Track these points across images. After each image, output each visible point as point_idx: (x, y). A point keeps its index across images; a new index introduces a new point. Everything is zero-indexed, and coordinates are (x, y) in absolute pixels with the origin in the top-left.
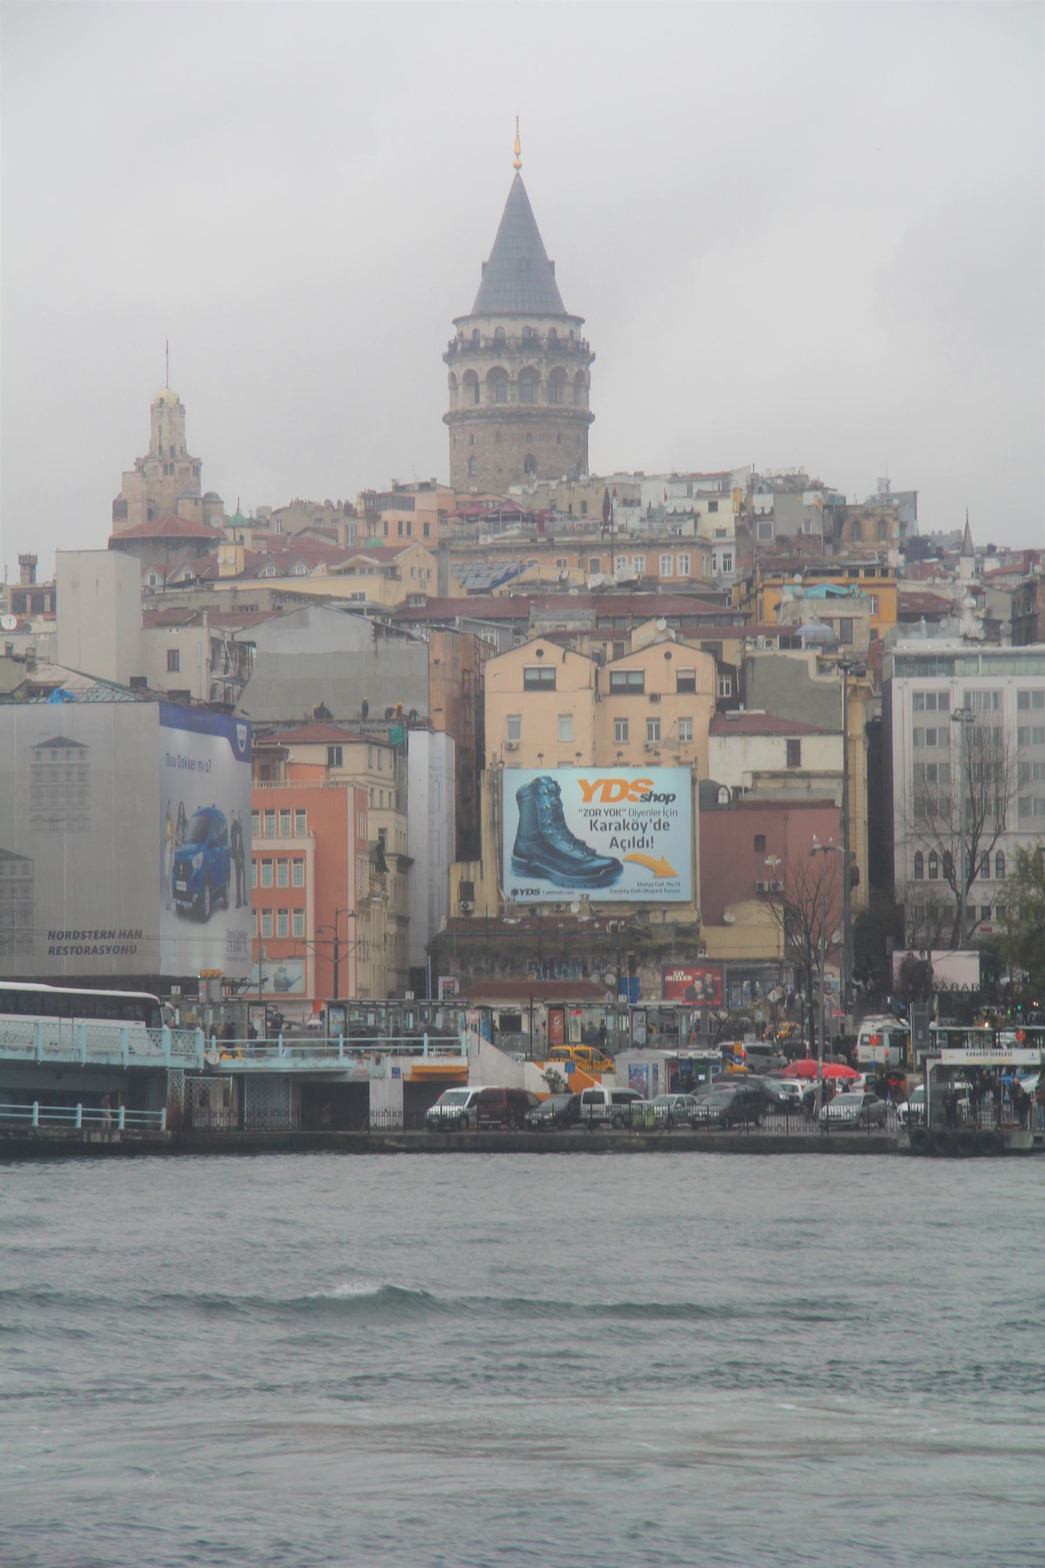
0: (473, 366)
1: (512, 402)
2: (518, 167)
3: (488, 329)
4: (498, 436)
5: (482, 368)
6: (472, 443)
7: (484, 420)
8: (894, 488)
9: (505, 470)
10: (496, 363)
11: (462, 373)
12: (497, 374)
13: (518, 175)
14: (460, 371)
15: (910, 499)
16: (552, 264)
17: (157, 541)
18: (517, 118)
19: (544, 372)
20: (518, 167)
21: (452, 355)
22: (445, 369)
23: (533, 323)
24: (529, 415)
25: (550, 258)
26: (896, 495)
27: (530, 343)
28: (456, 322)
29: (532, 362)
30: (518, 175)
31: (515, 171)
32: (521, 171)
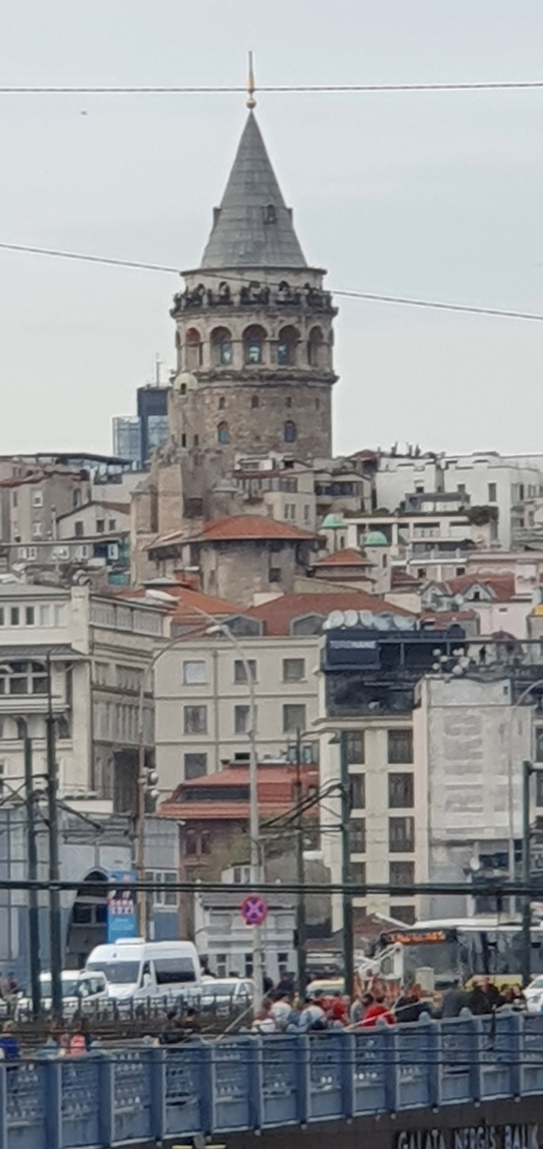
0: (225, 325)
2: (251, 106)
6: (221, 407)
7: (240, 383)
9: (263, 438)
10: (253, 320)
11: (210, 330)
13: (251, 117)
16: (290, 211)
17: (260, 543)
18: (250, 53)
20: (251, 106)
24: (291, 378)
25: (288, 205)
28: (184, 274)
29: (291, 321)
30: (251, 117)
31: (248, 110)
32: (255, 110)
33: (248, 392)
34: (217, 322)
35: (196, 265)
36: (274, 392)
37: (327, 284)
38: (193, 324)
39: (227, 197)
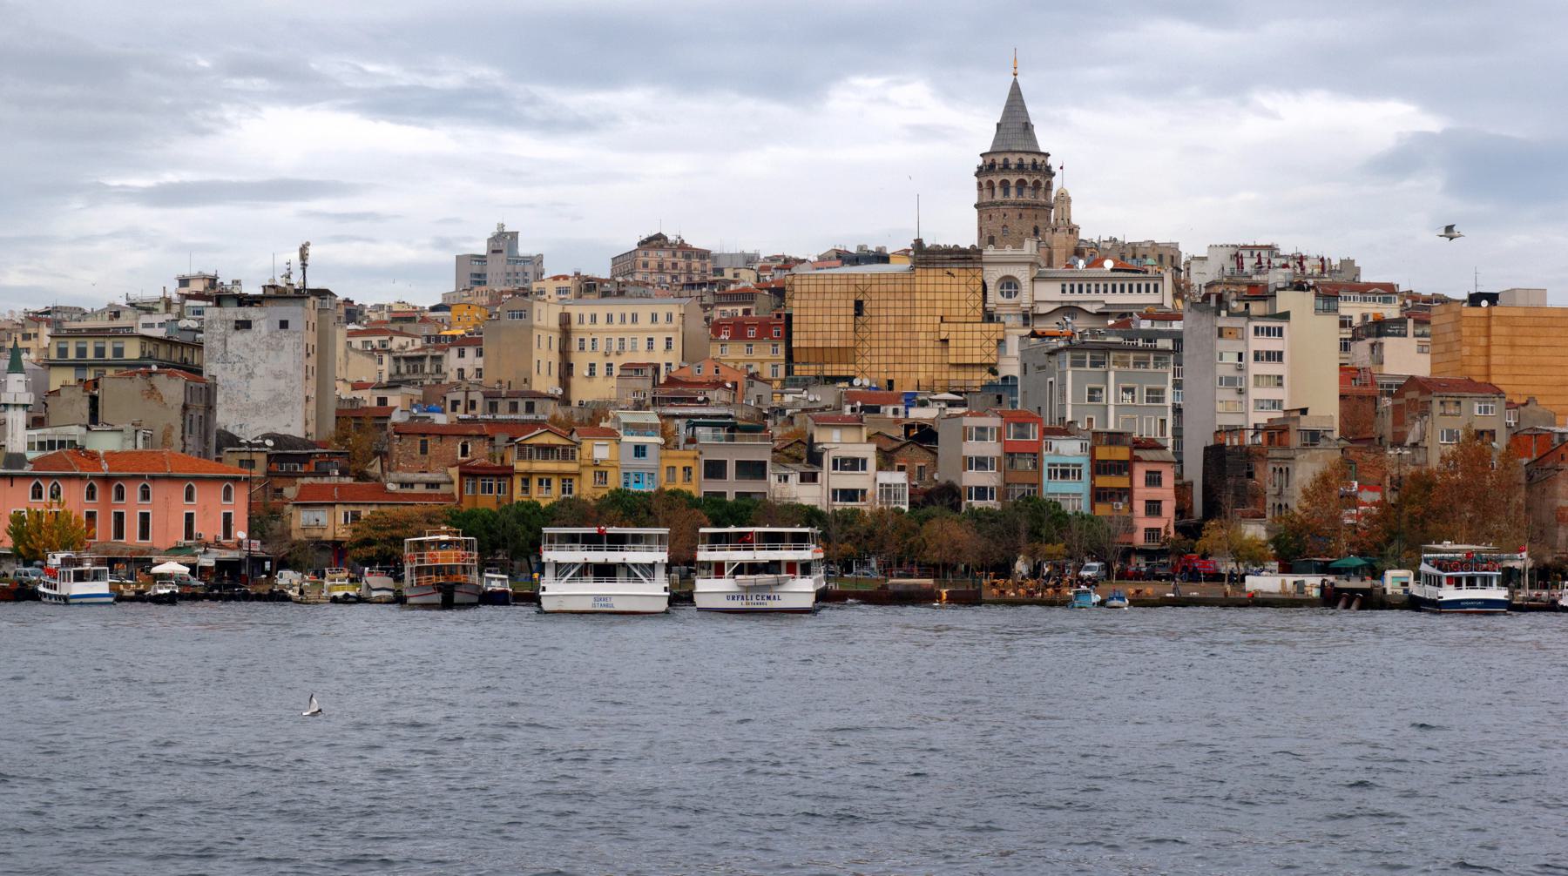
0: (1007, 178)
1: (1028, 196)
2: (1015, 75)
3: (999, 160)
4: (1021, 215)
5: (1013, 179)
8: (507, 229)
10: (1021, 177)
12: (1021, 183)
14: (984, 181)
15: (514, 235)
19: (1043, 185)
20: (1015, 75)
21: (980, 172)
22: (976, 179)
23: (1036, 157)
24: (1037, 205)
26: (507, 233)
27: (1020, 167)
28: (981, 155)
29: (1038, 178)
33: (1017, 212)
34: (1002, 177)
35: (988, 150)
36: (1029, 212)
37: (1050, 161)
38: (990, 178)
39: (1003, 118)
